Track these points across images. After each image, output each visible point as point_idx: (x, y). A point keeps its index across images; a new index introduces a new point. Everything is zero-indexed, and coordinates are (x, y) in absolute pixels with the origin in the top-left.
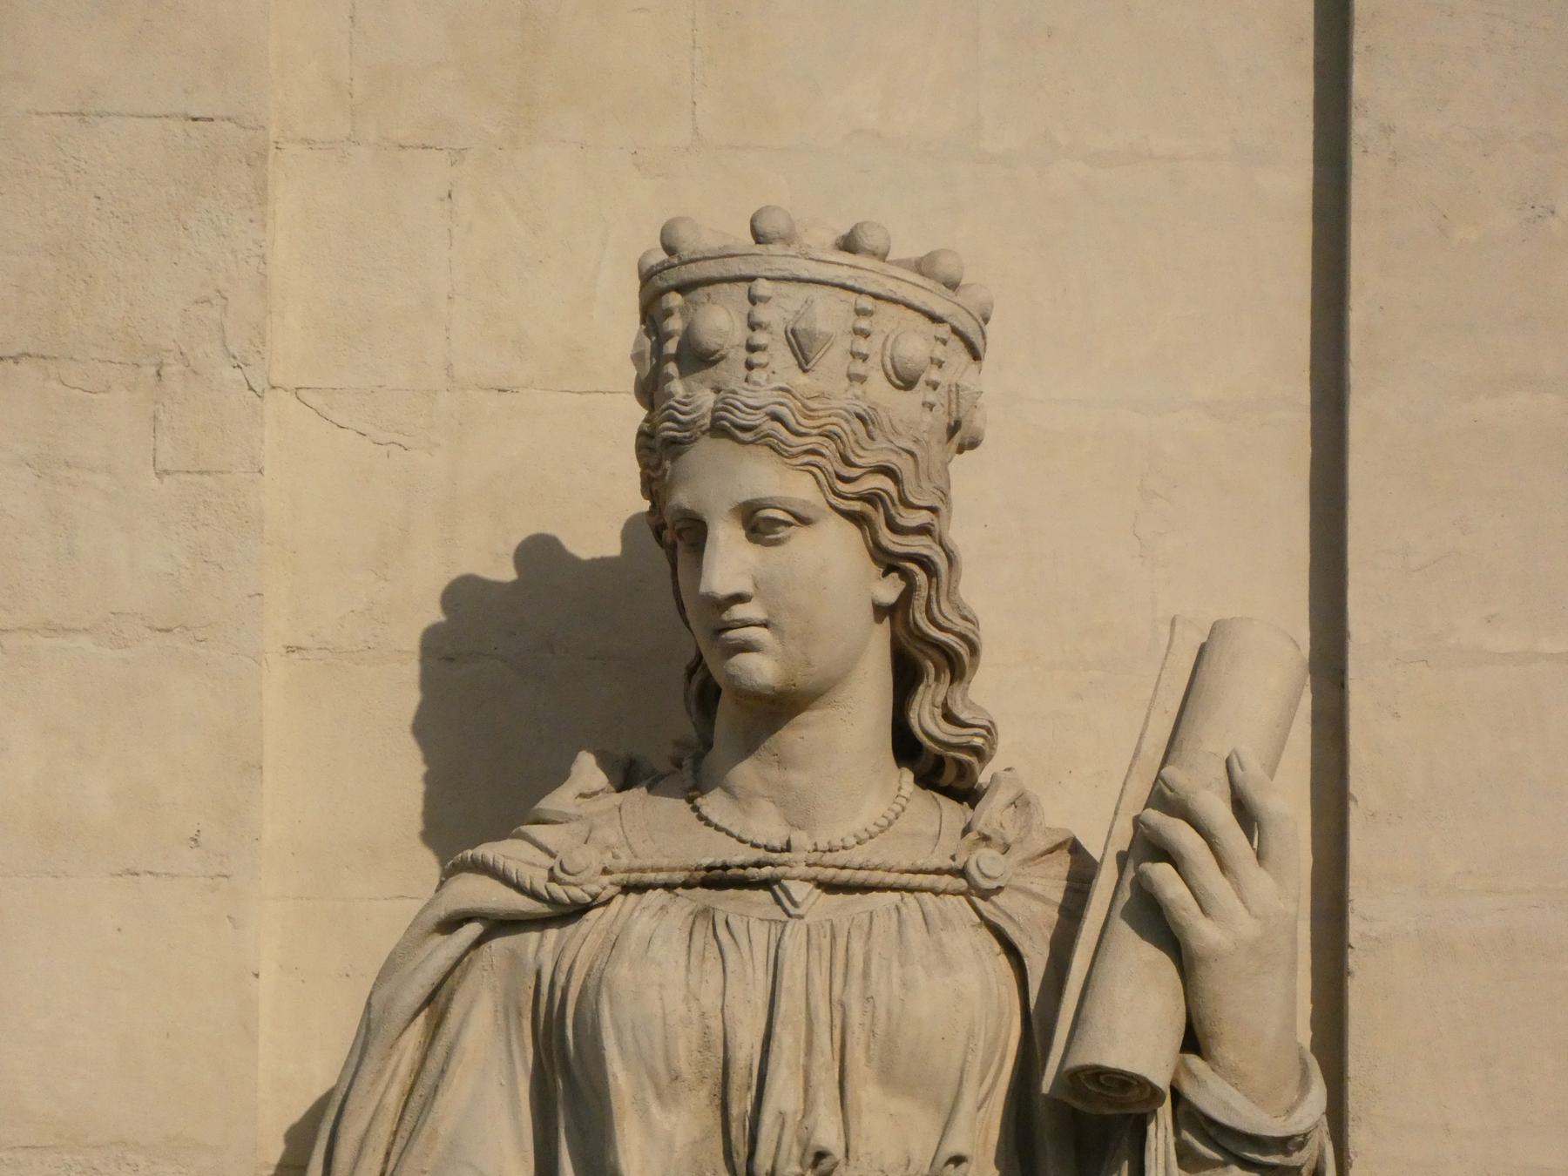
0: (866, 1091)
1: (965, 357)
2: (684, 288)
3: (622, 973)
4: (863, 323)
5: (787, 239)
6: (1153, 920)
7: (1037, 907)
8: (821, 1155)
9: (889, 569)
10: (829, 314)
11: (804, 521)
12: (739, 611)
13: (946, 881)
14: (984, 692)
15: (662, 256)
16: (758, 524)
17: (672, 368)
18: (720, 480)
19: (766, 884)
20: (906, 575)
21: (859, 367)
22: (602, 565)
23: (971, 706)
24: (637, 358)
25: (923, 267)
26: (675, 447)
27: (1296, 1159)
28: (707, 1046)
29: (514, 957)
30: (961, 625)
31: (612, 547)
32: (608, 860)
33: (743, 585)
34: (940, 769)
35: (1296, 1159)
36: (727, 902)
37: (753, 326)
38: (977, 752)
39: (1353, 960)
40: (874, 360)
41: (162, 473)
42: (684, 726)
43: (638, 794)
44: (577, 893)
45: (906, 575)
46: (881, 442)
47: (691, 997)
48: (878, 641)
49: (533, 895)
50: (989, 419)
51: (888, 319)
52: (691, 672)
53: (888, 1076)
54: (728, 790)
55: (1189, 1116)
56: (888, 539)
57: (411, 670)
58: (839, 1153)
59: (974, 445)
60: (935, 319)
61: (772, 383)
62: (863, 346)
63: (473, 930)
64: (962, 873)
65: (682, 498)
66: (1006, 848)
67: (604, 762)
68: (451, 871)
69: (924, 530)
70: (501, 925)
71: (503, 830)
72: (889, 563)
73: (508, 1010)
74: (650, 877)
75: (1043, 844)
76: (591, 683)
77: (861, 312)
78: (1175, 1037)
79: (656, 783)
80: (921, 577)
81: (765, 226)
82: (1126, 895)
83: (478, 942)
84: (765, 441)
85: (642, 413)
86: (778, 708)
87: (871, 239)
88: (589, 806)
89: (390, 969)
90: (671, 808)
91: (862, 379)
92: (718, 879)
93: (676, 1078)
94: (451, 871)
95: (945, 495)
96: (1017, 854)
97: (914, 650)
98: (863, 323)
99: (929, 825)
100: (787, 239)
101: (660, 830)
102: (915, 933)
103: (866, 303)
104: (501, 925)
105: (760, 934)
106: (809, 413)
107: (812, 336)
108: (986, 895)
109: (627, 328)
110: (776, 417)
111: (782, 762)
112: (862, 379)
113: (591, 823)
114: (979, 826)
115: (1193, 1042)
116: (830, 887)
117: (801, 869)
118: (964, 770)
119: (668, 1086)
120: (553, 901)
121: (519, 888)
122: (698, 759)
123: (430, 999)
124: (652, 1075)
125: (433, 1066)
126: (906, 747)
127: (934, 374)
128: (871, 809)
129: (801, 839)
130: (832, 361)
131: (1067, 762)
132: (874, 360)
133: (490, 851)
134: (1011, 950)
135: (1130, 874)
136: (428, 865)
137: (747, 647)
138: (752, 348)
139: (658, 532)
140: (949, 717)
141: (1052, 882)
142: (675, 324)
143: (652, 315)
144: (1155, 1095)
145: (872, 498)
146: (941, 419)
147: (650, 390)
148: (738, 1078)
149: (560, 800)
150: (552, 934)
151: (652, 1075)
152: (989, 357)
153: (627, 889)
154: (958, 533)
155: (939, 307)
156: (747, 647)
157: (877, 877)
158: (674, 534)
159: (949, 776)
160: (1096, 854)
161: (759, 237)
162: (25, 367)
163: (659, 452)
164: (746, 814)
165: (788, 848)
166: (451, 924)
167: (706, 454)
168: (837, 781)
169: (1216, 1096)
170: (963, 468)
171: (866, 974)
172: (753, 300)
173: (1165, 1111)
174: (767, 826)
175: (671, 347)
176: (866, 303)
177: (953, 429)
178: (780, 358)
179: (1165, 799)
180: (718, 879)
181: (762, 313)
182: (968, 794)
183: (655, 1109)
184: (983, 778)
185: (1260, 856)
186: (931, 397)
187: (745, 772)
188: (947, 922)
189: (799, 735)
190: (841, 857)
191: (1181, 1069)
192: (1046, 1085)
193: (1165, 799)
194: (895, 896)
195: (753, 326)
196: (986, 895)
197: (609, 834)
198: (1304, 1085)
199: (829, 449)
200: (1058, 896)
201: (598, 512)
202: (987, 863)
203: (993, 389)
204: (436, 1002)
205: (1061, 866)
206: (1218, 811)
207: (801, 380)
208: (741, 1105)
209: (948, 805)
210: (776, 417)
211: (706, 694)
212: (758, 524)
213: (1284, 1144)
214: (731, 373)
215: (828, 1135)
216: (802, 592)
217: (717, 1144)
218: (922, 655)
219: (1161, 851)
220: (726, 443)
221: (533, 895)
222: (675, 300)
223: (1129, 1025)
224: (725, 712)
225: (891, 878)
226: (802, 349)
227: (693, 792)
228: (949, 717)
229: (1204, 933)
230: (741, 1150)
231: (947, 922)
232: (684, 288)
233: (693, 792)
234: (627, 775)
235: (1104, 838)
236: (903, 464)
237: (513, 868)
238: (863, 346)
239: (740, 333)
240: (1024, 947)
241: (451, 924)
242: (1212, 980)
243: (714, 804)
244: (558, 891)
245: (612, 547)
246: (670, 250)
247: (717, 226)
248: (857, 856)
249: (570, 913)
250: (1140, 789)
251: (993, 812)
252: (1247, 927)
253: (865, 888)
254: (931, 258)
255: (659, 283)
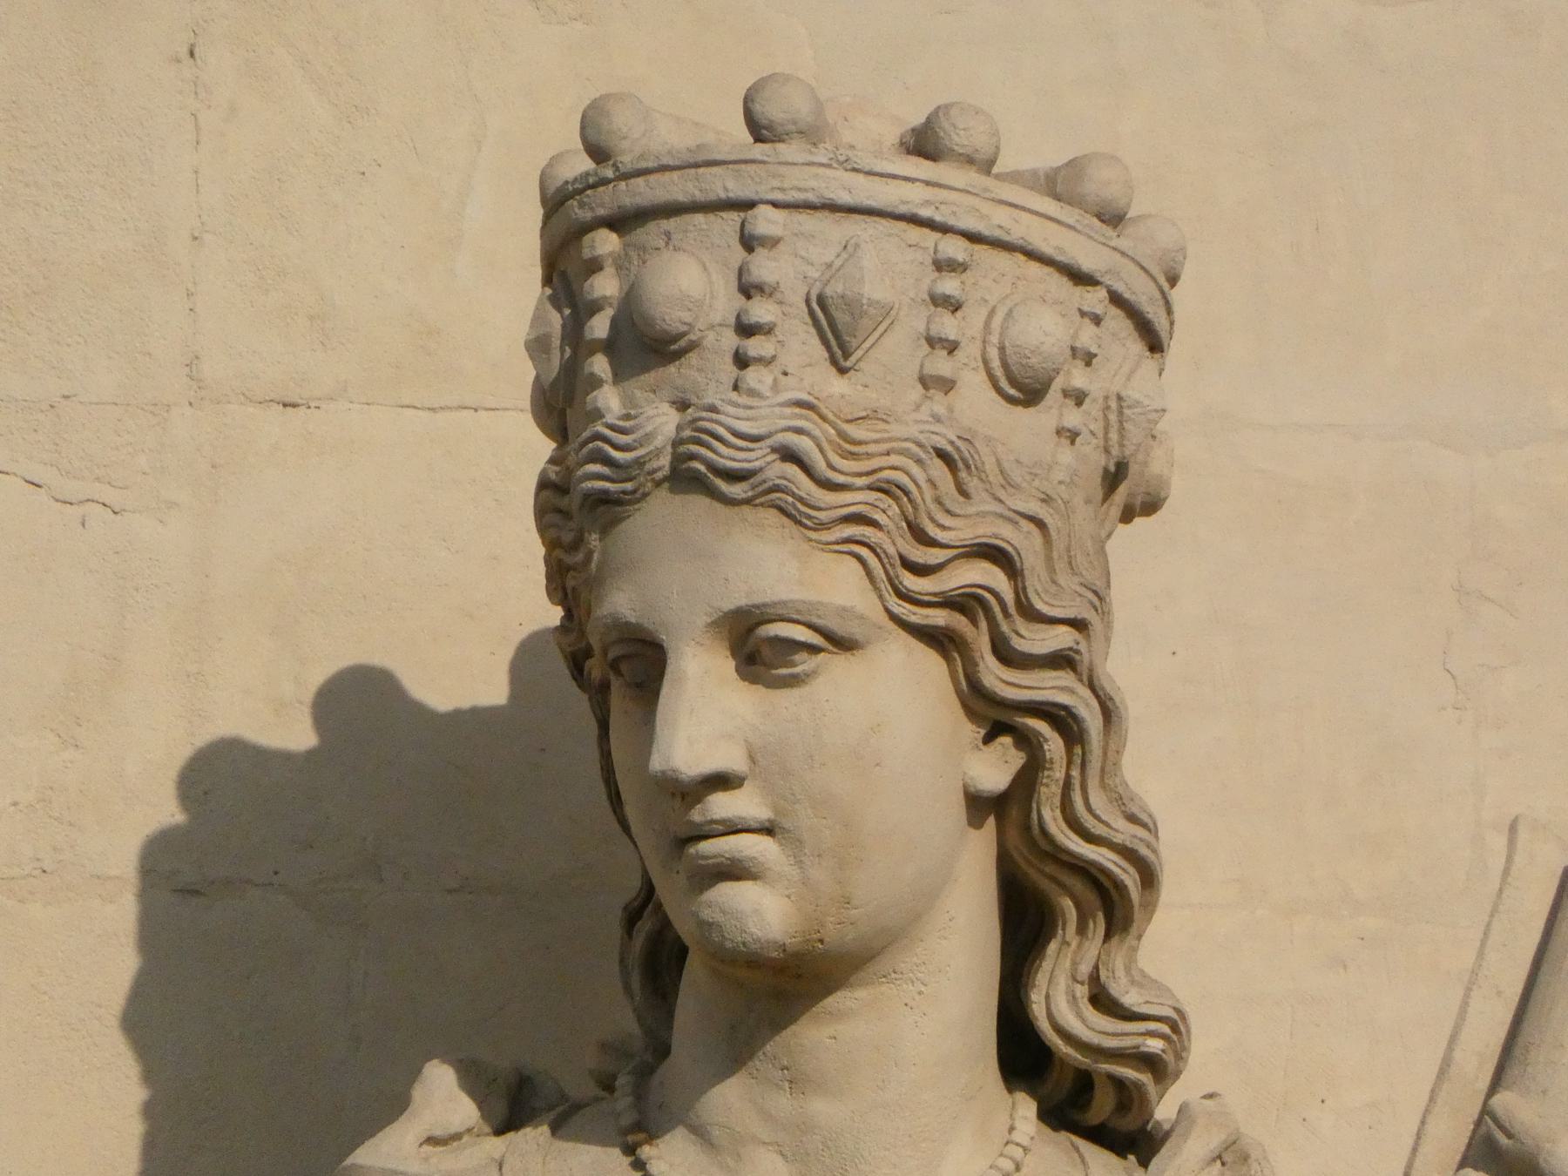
1: (1137, 347)
2: (621, 222)
4: (949, 285)
5: (811, 134)
10: (886, 269)
11: (843, 644)
12: (722, 805)
14: (1170, 958)
15: (585, 164)
16: (756, 647)
17: (600, 365)
18: (689, 568)
20: (1026, 741)
21: (941, 365)
23: (1142, 981)
24: (537, 347)
25: (1058, 184)
26: (607, 509)
30: (1124, 832)
31: (493, 691)
37: (748, 290)
38: (1151, 1063)
40: (969, 351)
42: (621, 1017)
43: (534, 1137)
45: (1026, 741)
50: (1180, 460)
52: (632, 917)
54: (700, 1132)
56: (995, 676)
59: (1151, 506)
60: (1080, 278)
65: (621, 602)
67: (474, 1079)
69: (1062, 661)
72: (995, 719)
77: (944, 266)
79: (565, 1118)
80: (1054, 745)
85: (547, 447)
86: (792, 982)
87: (963, 134)
91: (947, 385)
95: (1100, 598)
97: (1038, 876)
98: (949, 285)
100: (811, 134)
103: (954, 248)
106: (850, 447)
107: (854, 306)
109: (514, 296)
110: (789, 455)
111: (796, 1081)
112: (947, 385)
118: (1129, 1098)
122: (645, 1073)
126: (1022, 1054)
127: (1079, 378)
130: (892, 356)
132: (969, 351)
137: (734, 871)
138: (746, 330)
139: (577, 663)
140: (1102, 1000)
142: (605, 286)
143: (563, 267)
145: (966, 603)
146: (1090, 459)
147: (559, 405)
152: (1176, 349)
154: (1124, 665)
155: (1087, 261)
156: (734, 871)
158: (607, 667)
159: (1102, 1107)
161: (759, 130)
163: (578, 517)
167: (663, 520)
170: (1130, 545)
172: (749, 243)
175: (599, 327)
176: (954, 248)
177: (1114, 478)
178: (798, 346)
181: (764, 267)
184: (1164, 1111)
186: (1073, 418)
187: (730, 1100)
189: (832, 1032)
199: (888, 512)
203: (1186, 404)
207: (837, 386)
210: (789, 455)
211: (660, 957)
214: (707, 372)
216: (836, 774)
218: (1056, 887)
220: (700, 502)
222: (606, 243)
227: (635, 1135)
228: (1102, 1000)
232: (621, 222)
234: (513, 1104)
238: (948, 326)
245: (493, 691)
246: (598, 153)
247: (683, 110)
255: (579, 212)
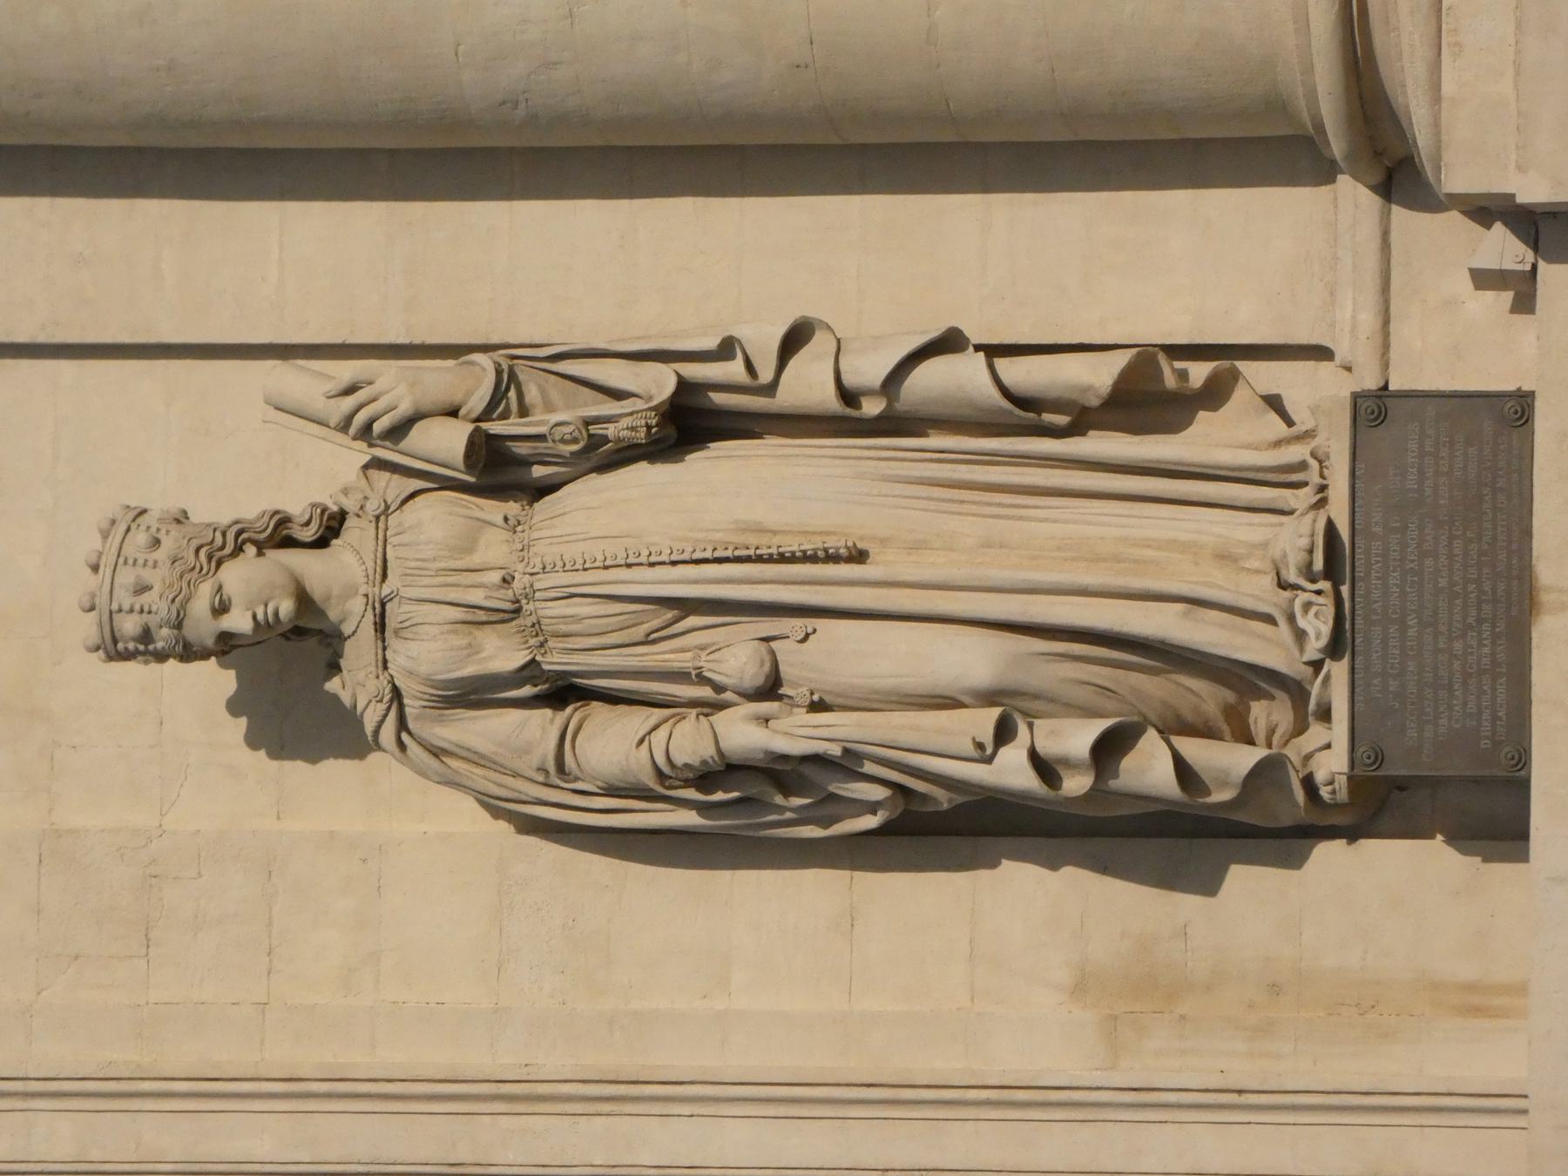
0: (476, 560)
1: (145, 516)
2: (115, 642)
3: (424, 669)
4: (131, 561)
5: (93, 596)
6: (398, 431)
7: (393, 484)
8: (504, 580)
9: (241, 550)
10: (126, 577)
11: (220, 588)
12: (260, 617)
13: (381, 525)
14: (296, 507)
15: (101, 652)
16: (221, 609)
17: (151, 647)
18: (202, 626)
19: (383, 605)
20: (244, 542)
21: (150, 563)
22: (239, 678)
23: (302, 514)
24: (146, 662)
25: (105, 535)
26: (187, 646)
27: (505, 367)
28: (455, 632)
29: (417, 718)
30: (266, 518)
31: (232, 673)
32: (372, 676)
33: (249, 615)
34: (331, 527)
35: (505, 367)
36: (391, 623)
37: (132, 611)
38: (323, 512)
39: (417, 341)
40: (148, 556)
41: (200, 875)
42: (312, 642)
43: (343, 663)
44: (387, 691)
45: (244, 542)
46: (185, 554)
47: (434, 639)
48: (275, 555)
49: (389, 709)
50: (174, 504)
51: (128, 550)
52: (288, 639)
53: (469, 549)
54: (341, 622)
55: (486, 415)
56: (228, 551)
57: (288, 765)
58: (503, 572)
59: (185, 512)
60: (128, 530)
61: (158, 603)
62: (141, 562)
63: (404, 736)
64: (377, 518)
65: (210, 642)
66: (366, 498)
67: (328, 678)
68: (377, 746)
69: (224, 534)
70: (402, 724)
71: (359, 722)
72: (238, 550)
73: (440, 720)
74: (380, 657)
75: (364, 481)
76: (293, 683)
77: (126, 562)
78: (450, 421)
79: (338, 654)
80: (245, 536)
81: (88, 605)
82: (387, 443)
83: (409, 733)
84: (184, 606)
85: (171, 661)
86: (304, 600)
87: (93, 559)
88: (348, 684)
89: (423, 773)
90: (349, 647)
91: (156, 562)
92: (381, 626)
93: (470, 645)
94: (377, 746)
95: (209, 525)
96: (368, 493)
97: (278, 538)
98: (131, 561)
99: (357, 534)
100: (93, 596)
101: (359, 653)
102: (405, 538)
103: (121, 560)
104: (402, 724)
105: (405, 608)
106: (171, 585)
107: (137, 584)
108: (387, 507)
109: (133, 668)
110: (173, 601)
111: (328, 598)
112: (156, 562)
113: (356, 684)
114: (356, 510)
115: (453, 413)
116: (384, 576)
117: (376, 589)
118: (332, 517)
119: (473, 650)
120: (391, 701)
121: (385, 716)
122: (327, 636)
123: (436, 756)
124: (469, 656)
125: (465, 754)
126: (321, 543)
127: (153, 529)
128: (349, 558)
129: (363, 590)
130: (148, 576)
131: (325, 471)
132: (148, 556)
133: (369, 728)
134: (412, 496)
135: (379, 442)
136: (374, 757)
137: (276, 614)
138: (142, 611)
139: (224, 653)
140: (308, 524)
141: (381, 478)
142: (131, 646)
143: (127, 656)
144: (477, 429)
145: (210, 558)
146: (174, 527)
147: (161, 657)
148: (470, 617)
149: (346, 698)
150: (406, 701)
151: (469, 656)
152: (145, 505)
153: (385, 668)
154: (225, 519)
155: (123, 528)
156: (276, 614)
157: (380, 555)
158: (226, 646)
159: (334, 524)
160: (368, 458)
161: (92, 609)
162: (151, 935)
163: (189, 652)
164: (353, 615)
165: (366, 596)
166: (402, 746)
167: (189, 631)
168: (336, 573)
169: (478, 401)
170: (194, 517)
171: (424, 560)
172: (120, 610)
173: (484, 425)
174: (357, 605)
175: (141, 648)
176: (121, 560)
177: (178, 521)
178: (146, 599)
179: (344, 426)
180: (381, 626)
181: (126, 607)
182: (342, 516)
183: (484, 655)
184: (335, 508)
185: (370, 383)
186: (163, 531)
187: (333, 614)
188: (400, 524)
189: (316, 590)
190: (371, 572)
191: (465, 418)
192: (472, 479)
193: (344, 426)
194: (389, 548)
195: (132, 611)
196: (387, 507)
197: (362, 674)
198: (473, 363)
199: (187, 577)
200: (388, 474)
201: (215, 681)
202: (373, 506)
203: (160, 502)
204: (437, 752)
205: (374, 474)
206: (349, 402)
207: (157, 589)
208: (482, 616)
209: (347, 524)
210: (173, 601)
211: (297, 632)
212: (221, 609)
213: (499, 372)
214: (153, 621)
215: (495, 577)
216: (252, 590)
217: (499, 627)
218: (280, 536)
219: (368, 428)
220: (185, 623)
221: (389, 709)
222: (120, 646)
223: (445, 442)
224: (305, 623)
225: (380, 549)
226: (142, 589)
227: (342, 638)
228: (308, 524)
229: (405, 408)
230: (501, 616)
231: (400, 524)
232: (115, 642)
233: (342, 638)
234: (334, 668)
235: (360, 454)
236: (195, 543)
237: (377, 718)
238: (141, 562)
239: (135, 617)
240: (411, 490)
241: (402, 746)
242: (427, 403)
243: (347, 629)
244: (387, 698)
245: (232, 673)
246: (98, 649)
247: (87, 627)
248: (370, 564)
249: (397, 694)
250: (340, 437)
251: (350, 504)
252: (402, 390)
253: (385, 561)
254: (101, 531)
255: (113, 653)
